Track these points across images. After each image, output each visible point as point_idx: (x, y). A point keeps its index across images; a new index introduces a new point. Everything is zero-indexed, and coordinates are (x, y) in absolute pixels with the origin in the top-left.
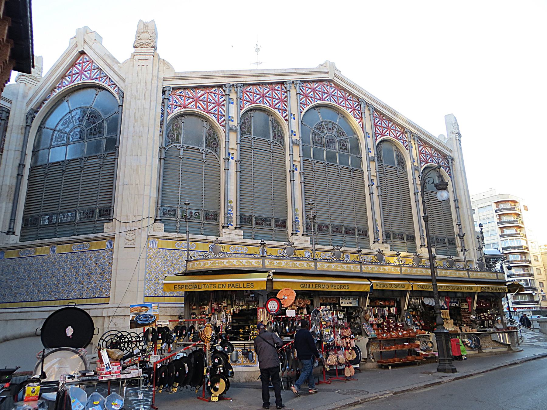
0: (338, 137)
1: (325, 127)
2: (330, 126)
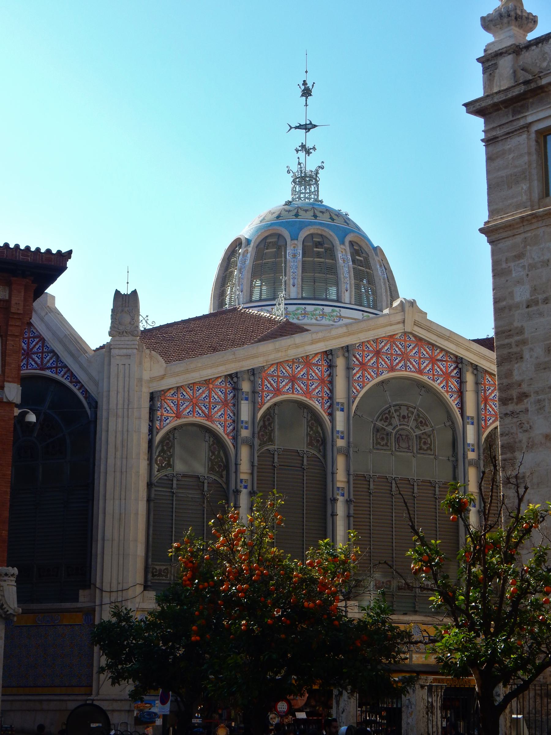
0: (416, 430)
1: (395, 415)
2: (404, 412)
